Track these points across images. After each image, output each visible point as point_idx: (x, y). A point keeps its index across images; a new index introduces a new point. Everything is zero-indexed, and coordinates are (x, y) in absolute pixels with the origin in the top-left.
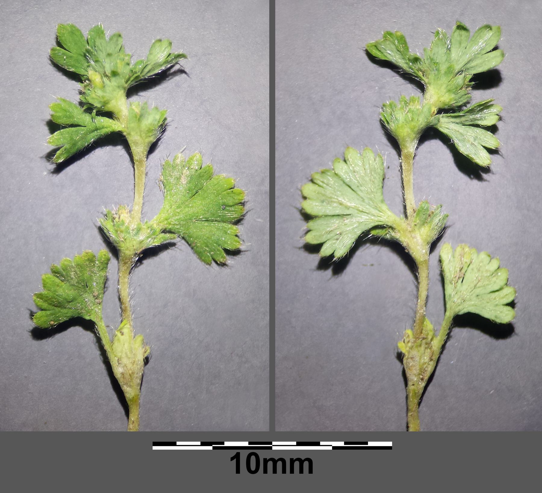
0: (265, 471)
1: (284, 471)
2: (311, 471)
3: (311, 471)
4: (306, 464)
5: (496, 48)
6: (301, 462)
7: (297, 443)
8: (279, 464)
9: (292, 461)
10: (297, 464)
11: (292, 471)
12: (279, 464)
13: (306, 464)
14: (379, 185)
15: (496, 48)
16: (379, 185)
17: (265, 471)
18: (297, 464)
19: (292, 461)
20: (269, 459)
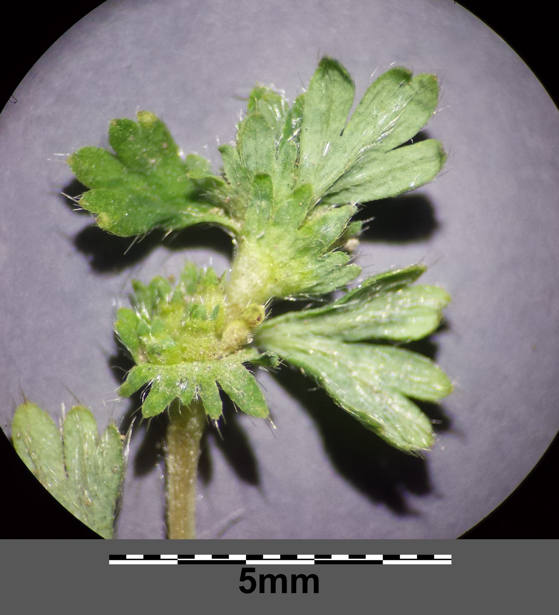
0: (262, 590)
1: (284, 590)
2: (316, 590)
3: (316, 590)
4: (311, 582)
5: (420, 137)
6: (305, 579)
7: (418, 556)
8: (279, 582)
9: (294, 578)
10: (300, 582)
11: (294, 590)
12: (279, 582)
13: (311, 582)
14: (105, 518)
15: (420, 137)
16: (105, 518)
17: (262, 590)
18: (300, 582)
19: (294, 578)
20: (266, 576)
